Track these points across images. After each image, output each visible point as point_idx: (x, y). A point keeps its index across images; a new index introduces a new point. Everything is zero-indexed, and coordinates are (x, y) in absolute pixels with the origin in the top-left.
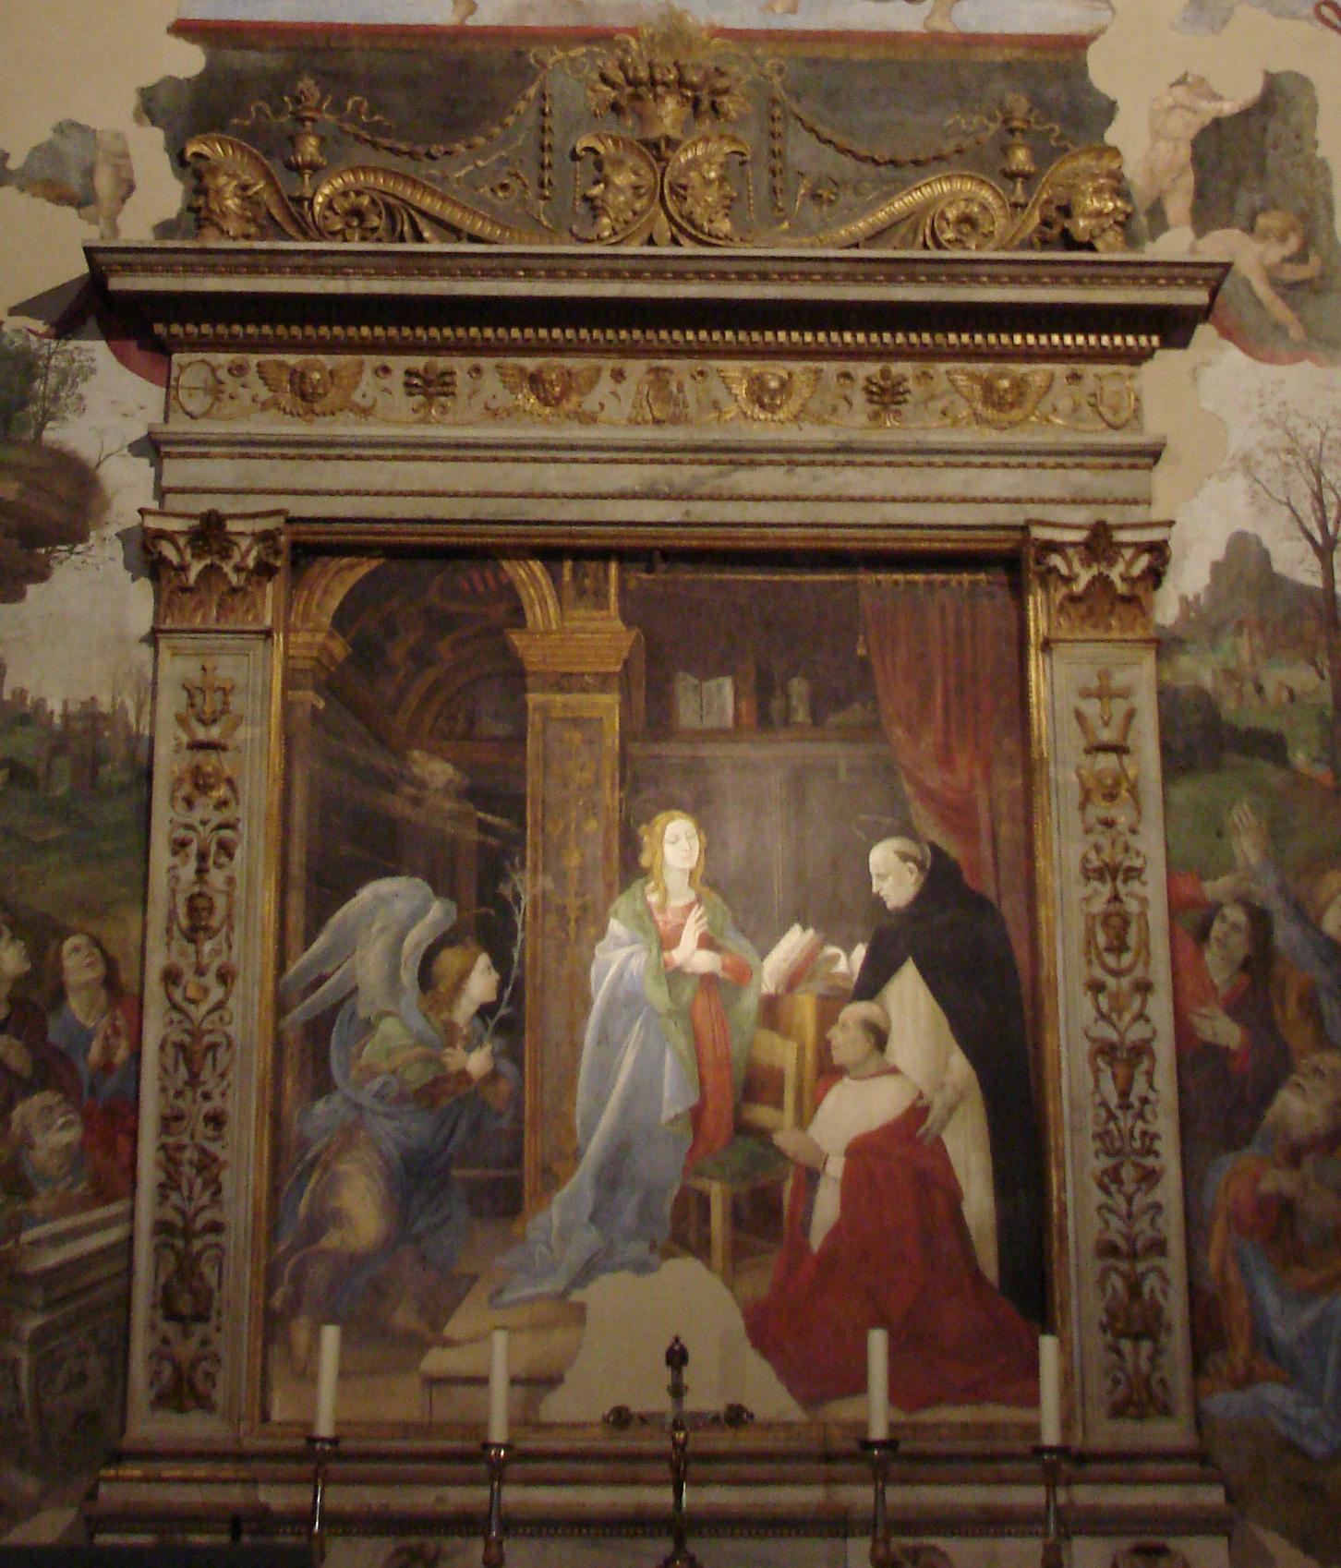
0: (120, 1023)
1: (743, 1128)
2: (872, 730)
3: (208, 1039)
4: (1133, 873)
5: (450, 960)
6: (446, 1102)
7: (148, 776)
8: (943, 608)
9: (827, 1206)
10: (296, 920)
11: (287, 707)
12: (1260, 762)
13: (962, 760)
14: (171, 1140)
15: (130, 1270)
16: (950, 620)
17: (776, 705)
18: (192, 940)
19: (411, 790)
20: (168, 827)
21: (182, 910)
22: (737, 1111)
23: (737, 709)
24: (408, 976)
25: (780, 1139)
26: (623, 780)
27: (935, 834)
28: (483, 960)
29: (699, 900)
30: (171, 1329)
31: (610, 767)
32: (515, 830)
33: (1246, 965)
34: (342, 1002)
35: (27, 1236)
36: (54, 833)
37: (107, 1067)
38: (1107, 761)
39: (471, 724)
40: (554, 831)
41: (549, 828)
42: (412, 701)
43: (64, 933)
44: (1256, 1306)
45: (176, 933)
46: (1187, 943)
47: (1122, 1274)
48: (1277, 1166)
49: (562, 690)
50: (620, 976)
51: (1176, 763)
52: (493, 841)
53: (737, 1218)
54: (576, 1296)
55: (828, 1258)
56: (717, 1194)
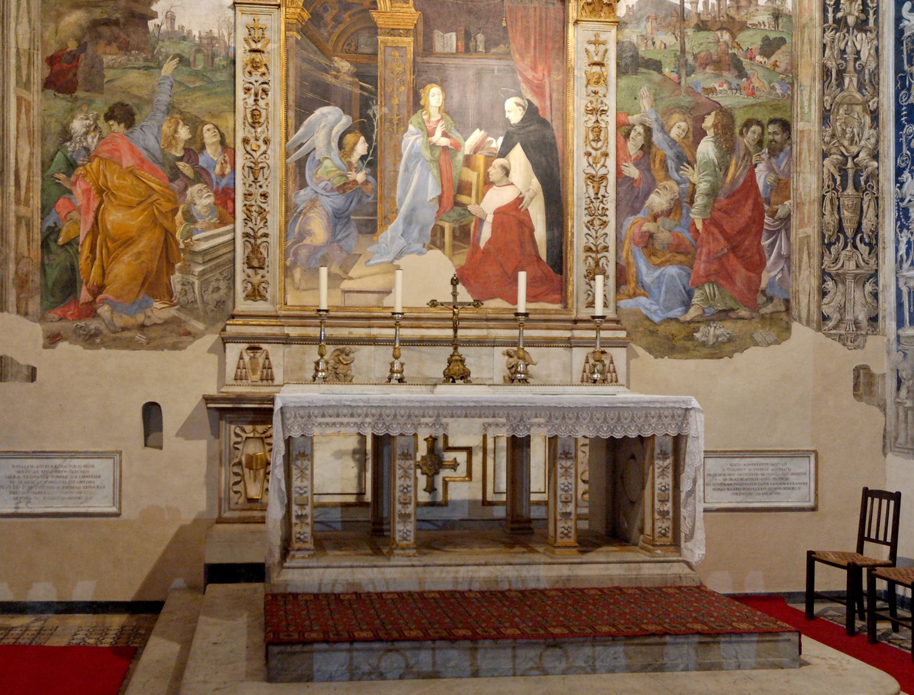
0: (227, 158)
1: (457, 204)
2: (507, 55)
3: (260, 165)
4: (603, 112)
5: (349, 138)
6: (349, 191)
7: (234, 62)
8: (535, 8)
9: (486, 233)
10: (292, 122)
11: (287, 38)
12: (651, 71)
13: (540, 68)
14: (248, 203)
15: (234, 250)
16: (538, 13)
17: (472, 44)
18: (254, 128)
19: (335, 73)
20: (242, 83)
21: (249, 116)
22: (455, 196)
23: (457, 46)
24: (334, 144)
25: (470, 208)
26: (414, 71)
27: (529, 96)
28: (362, 139)
29: (442, 118)
30: (250, 271)
31: (409, 66)
32: (373, 90)
33: (642, 148)
34: (308, 155)
35: (195, 237)
36: (198, 84)
37: (223, 175)
38: (596, 69)
39: (357, 47)
40: (388, 90)
41: (387, 89)
42: (334, 38)
43: (204, 123)
44: (638, 271)
45: (247, 124)
46: (622, 139)
47: (593, 258)
48: (649, 221)
49: (391, 35)
50: (413, 146)
51: (622, 71)
52: (366, 94)
53: (454, 237)
54: (396, 263)
55: (486, 252)
56: (447, 226)
